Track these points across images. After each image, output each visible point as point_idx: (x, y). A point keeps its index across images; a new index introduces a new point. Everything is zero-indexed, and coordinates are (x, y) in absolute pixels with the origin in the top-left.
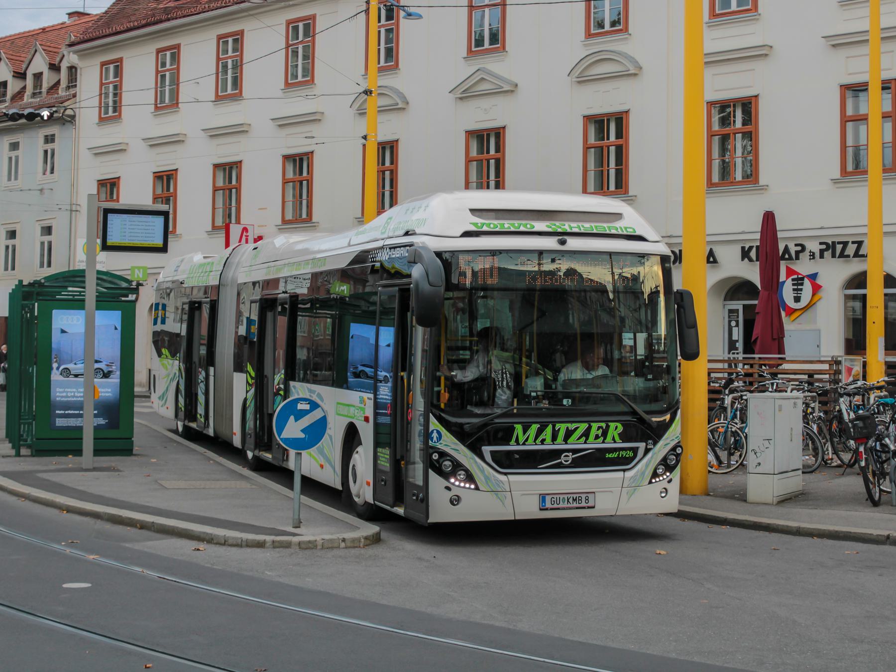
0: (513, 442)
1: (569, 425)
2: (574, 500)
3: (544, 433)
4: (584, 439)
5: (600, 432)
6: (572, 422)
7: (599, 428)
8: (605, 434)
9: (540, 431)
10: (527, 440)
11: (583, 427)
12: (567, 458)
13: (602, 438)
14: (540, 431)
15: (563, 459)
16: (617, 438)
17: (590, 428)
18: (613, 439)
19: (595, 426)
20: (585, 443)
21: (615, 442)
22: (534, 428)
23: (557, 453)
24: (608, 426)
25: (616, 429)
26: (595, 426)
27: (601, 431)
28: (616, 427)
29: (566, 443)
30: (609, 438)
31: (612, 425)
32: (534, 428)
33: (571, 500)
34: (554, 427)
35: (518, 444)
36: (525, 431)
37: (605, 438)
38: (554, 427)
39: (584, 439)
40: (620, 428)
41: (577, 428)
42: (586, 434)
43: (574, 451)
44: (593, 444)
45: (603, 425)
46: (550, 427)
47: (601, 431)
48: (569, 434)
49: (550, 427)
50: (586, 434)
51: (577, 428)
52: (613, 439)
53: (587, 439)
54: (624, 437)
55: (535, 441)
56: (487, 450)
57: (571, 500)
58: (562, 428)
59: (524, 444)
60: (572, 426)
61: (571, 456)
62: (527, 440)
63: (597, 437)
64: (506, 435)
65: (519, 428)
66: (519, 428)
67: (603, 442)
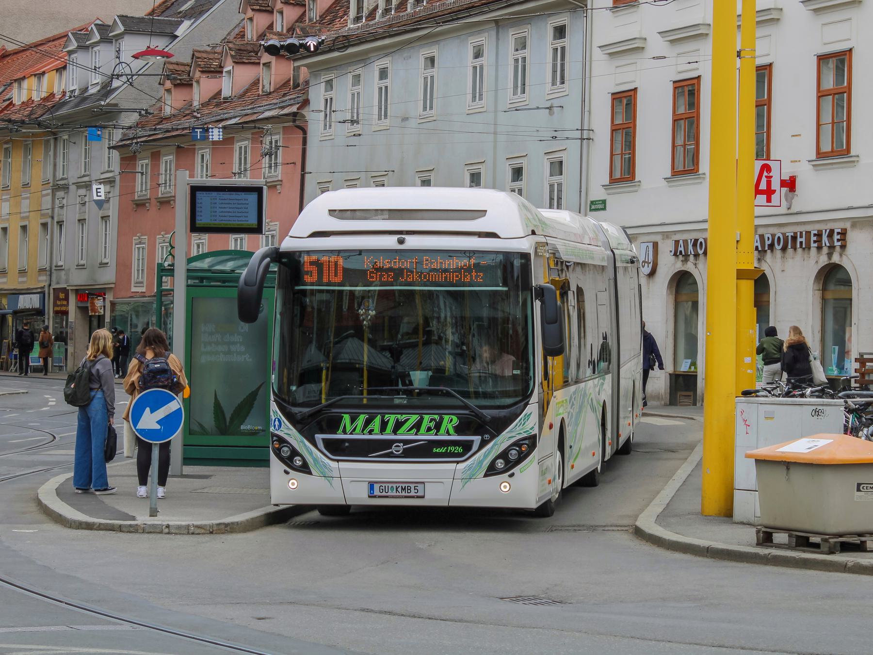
1: (399, 416)
5: (432, 425)
6: (402, 414)
8: (438, 426)
11: (414, 418)
16: (451, 431)
17: (422, 419)
20: (416, 434)
21: (449, 435)
22: (362, 418)
29: (396, 434)
32: (362, 418)
34: (383, 417)
36: (353, 420)
38: (383, 417)
39: (414, 430)
42: (417, 426)
44: (424, 436)
48: (398, 425)
50: (417, 426)
54: (458, 430)
58: (392, 419)
63: (429, 429)
64: (334, 424)
65: (347, 418)
66: (347, 418)
67: (436, 434)
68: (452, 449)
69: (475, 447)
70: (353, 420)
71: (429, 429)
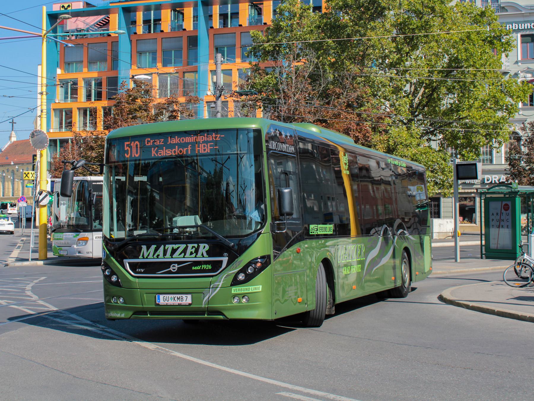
0: (141, 257)
2: (178, 299)
3: (159, 251)
4: (183, 254)
7: (193, 247)
8: (197, 251)
9: (156, 250)
10: (149, 255)
12: (174, 268)
13: (195, 254)
14: (156, 250)
15: (171, 269)
17: (187, 247)
18: (202, 255)
19: (190, 246)
20: (184, 257)
21: (203, 257)
22: (154, 247)
23: (168, 264)
24: (199, 246)
25: (204, 248)
27: (194, 249)
28: (205, 247)
29: (172, 258)
30: (199, 254)
31: (202, 245)
32: (154, 247)
33: (176, 299)
35: (144, 258)
36: (148, 249)
37: (197, 254)
39: (183, 254)
40: (207, 247)
41: (178, 248)
42: (185, 251)
43: (179, 263)
44: (189, 258)
45: (196, 245)
46: (163, 246)
47: (194, 249)
48: (174, 251)
49: (163, 246)
50: (185, 251)
51: (178, 248)
52: (202, 255)
53: (185, 255)
54: (209, 253)
55: (153, 256)
56: (126, 262)
57: (176, 299)
58: (170, 247)
59: (147, 258)
60: (175, 246)
62: (149, 255)
63: (191, 253)
65: (144, 247)
66: (144, 247)
67: (196, 257)
68: (204, 266)
69: (224, 265)
70: (148, 249)
71: (191, 253)
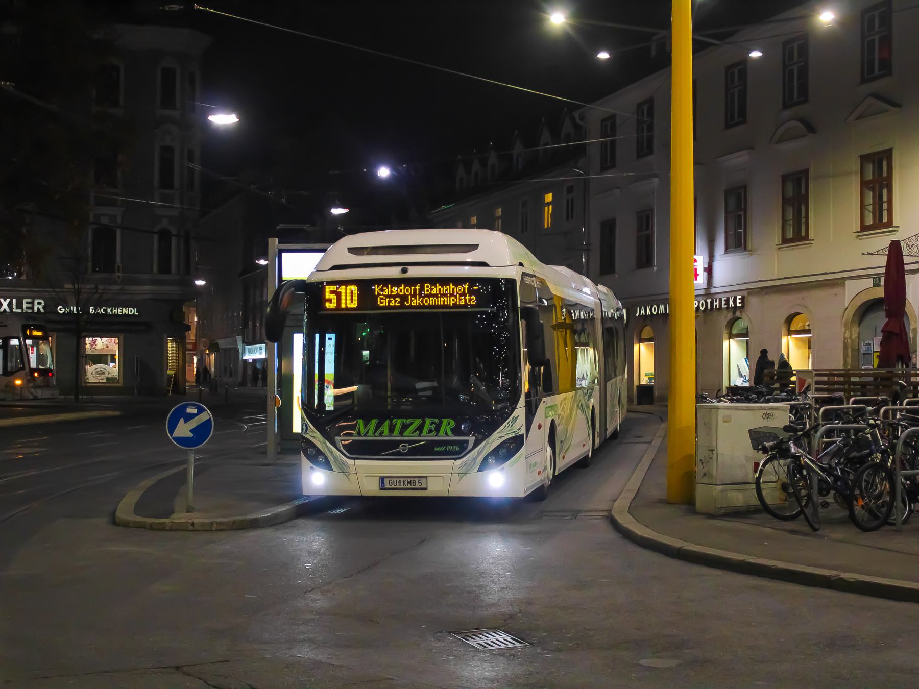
5: (433, 427)
7: (432, 423)
8: (438, 429)
9: (378, 426)
11: (417, 422)
14: (378, 426)
15: (400, 449)
16: (449, 433)
19: (428, 421)
22: (374, 422)
23: (396, 444)
24: (441, 423)
26: (428, 421)
31: (445, 421)
32: (374, 422)
33: (406, 483)
39: (417, 433)
42: (420, 428)
43: (411, 442)
44: (426, 437)
45: (436, 421)
48: (405, 427)
50: (420, 428)
51: (411, 424)
54: (456, 431)
57: (406, 483)
58: (399, 422)
59: (365, 435)
61: (408, 446)
63: (430, 431)
71: (430, 431)
